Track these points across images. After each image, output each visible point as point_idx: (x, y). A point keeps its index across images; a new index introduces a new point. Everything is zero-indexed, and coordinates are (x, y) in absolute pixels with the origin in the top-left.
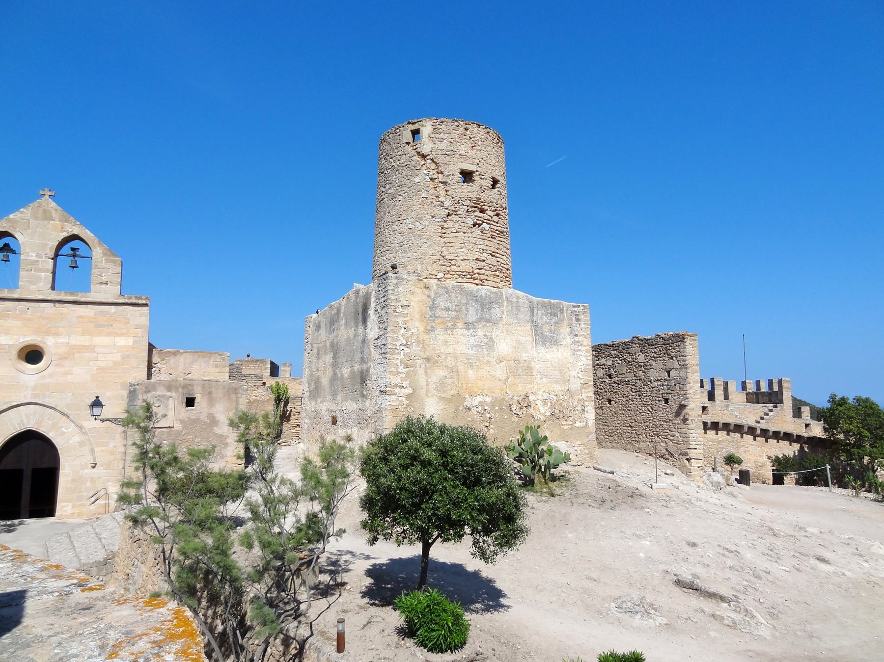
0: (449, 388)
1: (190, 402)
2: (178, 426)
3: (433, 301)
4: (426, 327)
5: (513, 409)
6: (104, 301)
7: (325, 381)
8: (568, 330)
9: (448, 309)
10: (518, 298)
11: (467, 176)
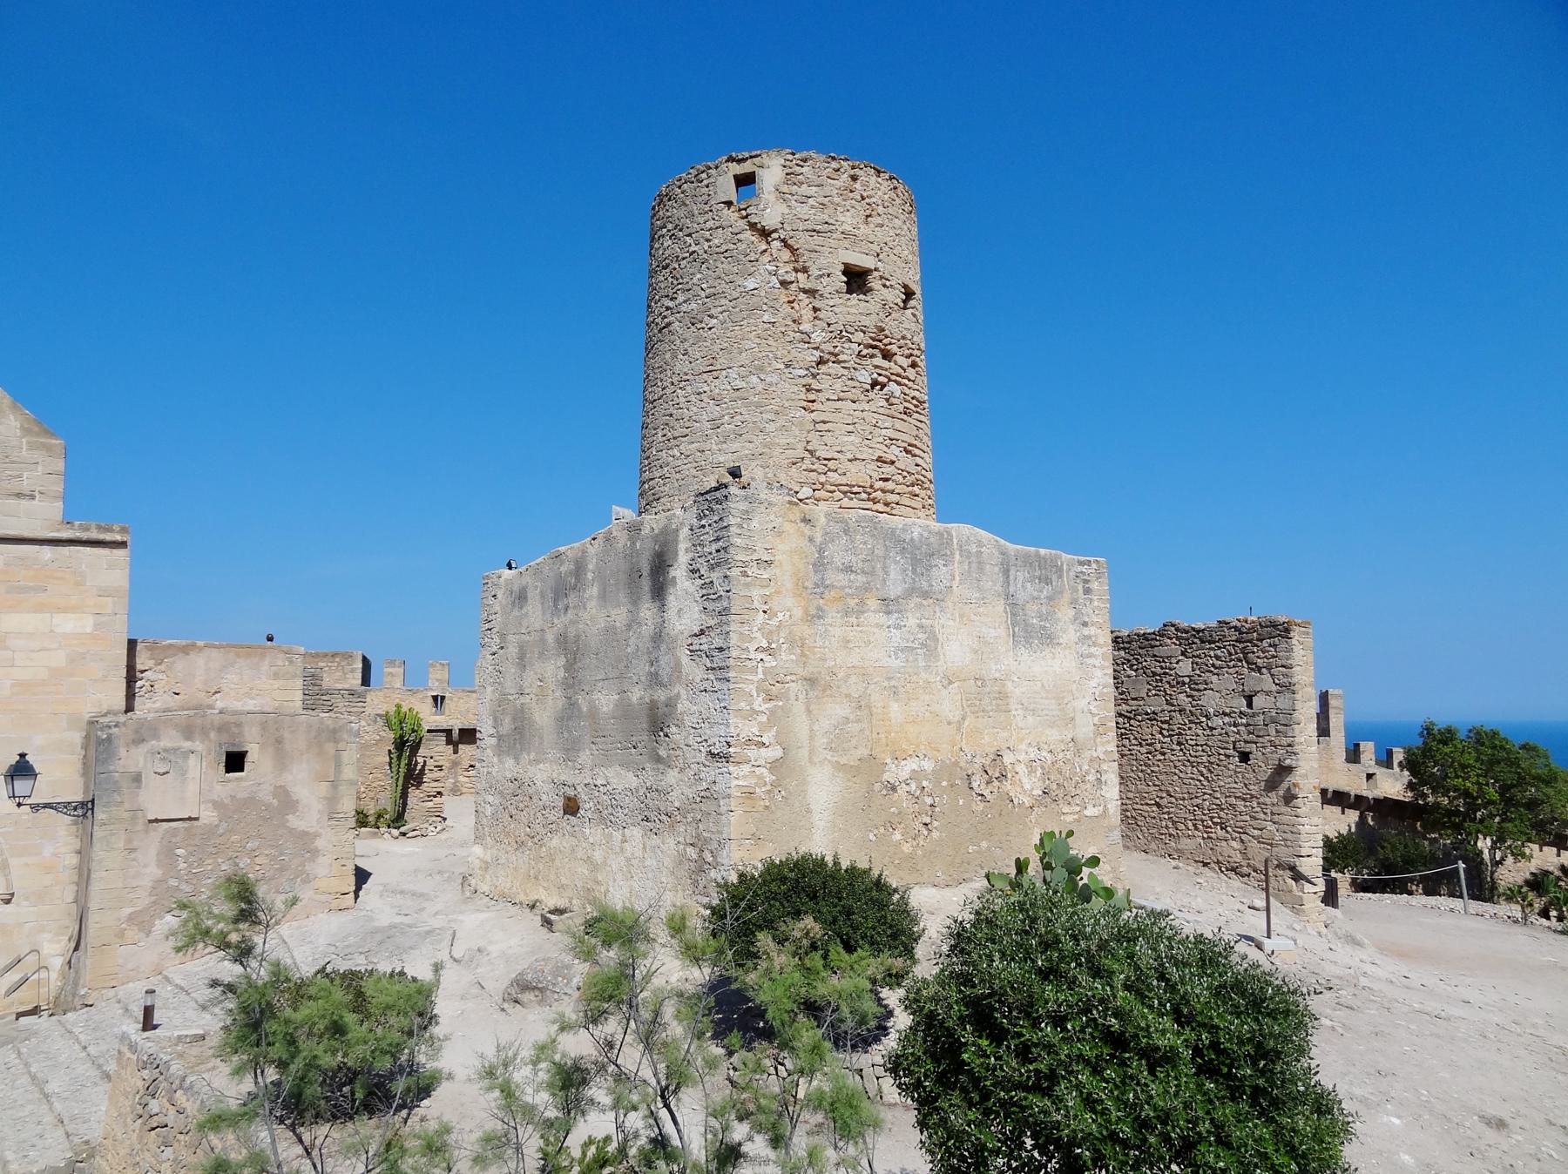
0: (854, 741)
1: (235, 762)
2: (208, 816)
3: (821, 551)
5: (975, 785)
6: (27, 534)
7: (543, 717)
8: (1071, 613)
9: (848, 569)
10: (980, 544)
11: (856, 279)
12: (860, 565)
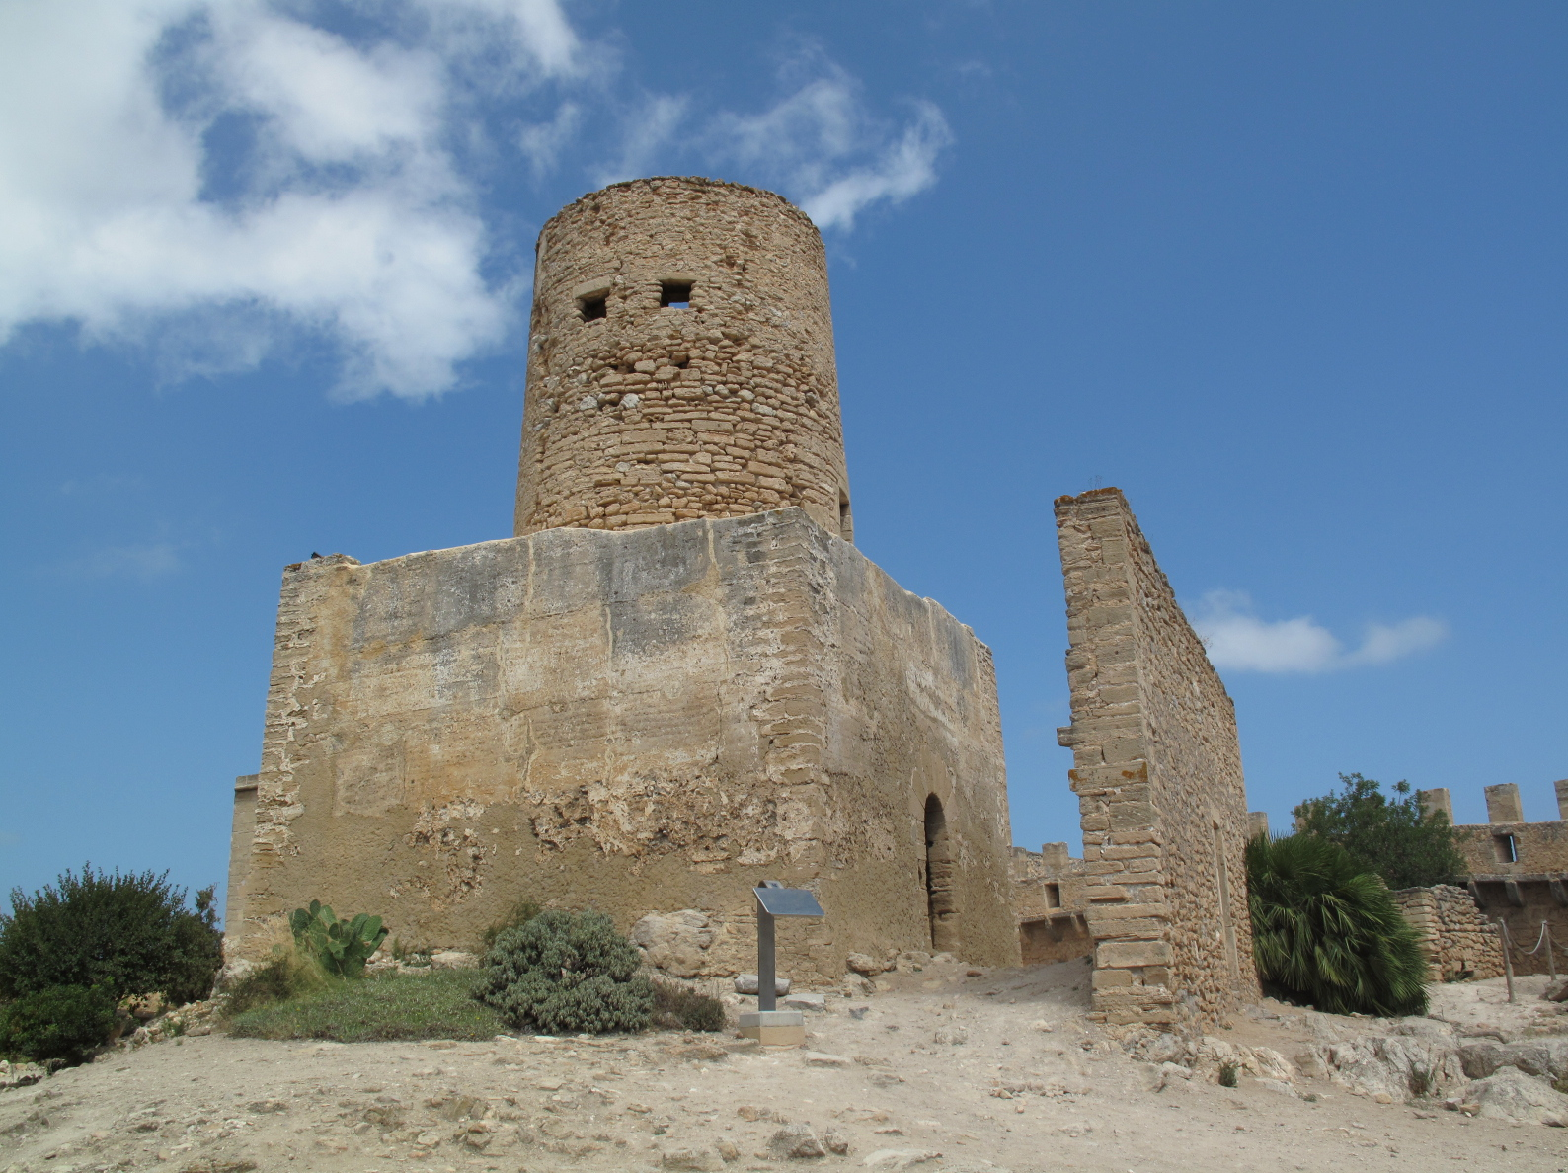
0: (381, 793)
3: (362, 607)
4: (342, 666)
5: (541, 830)
12: (407, 609)
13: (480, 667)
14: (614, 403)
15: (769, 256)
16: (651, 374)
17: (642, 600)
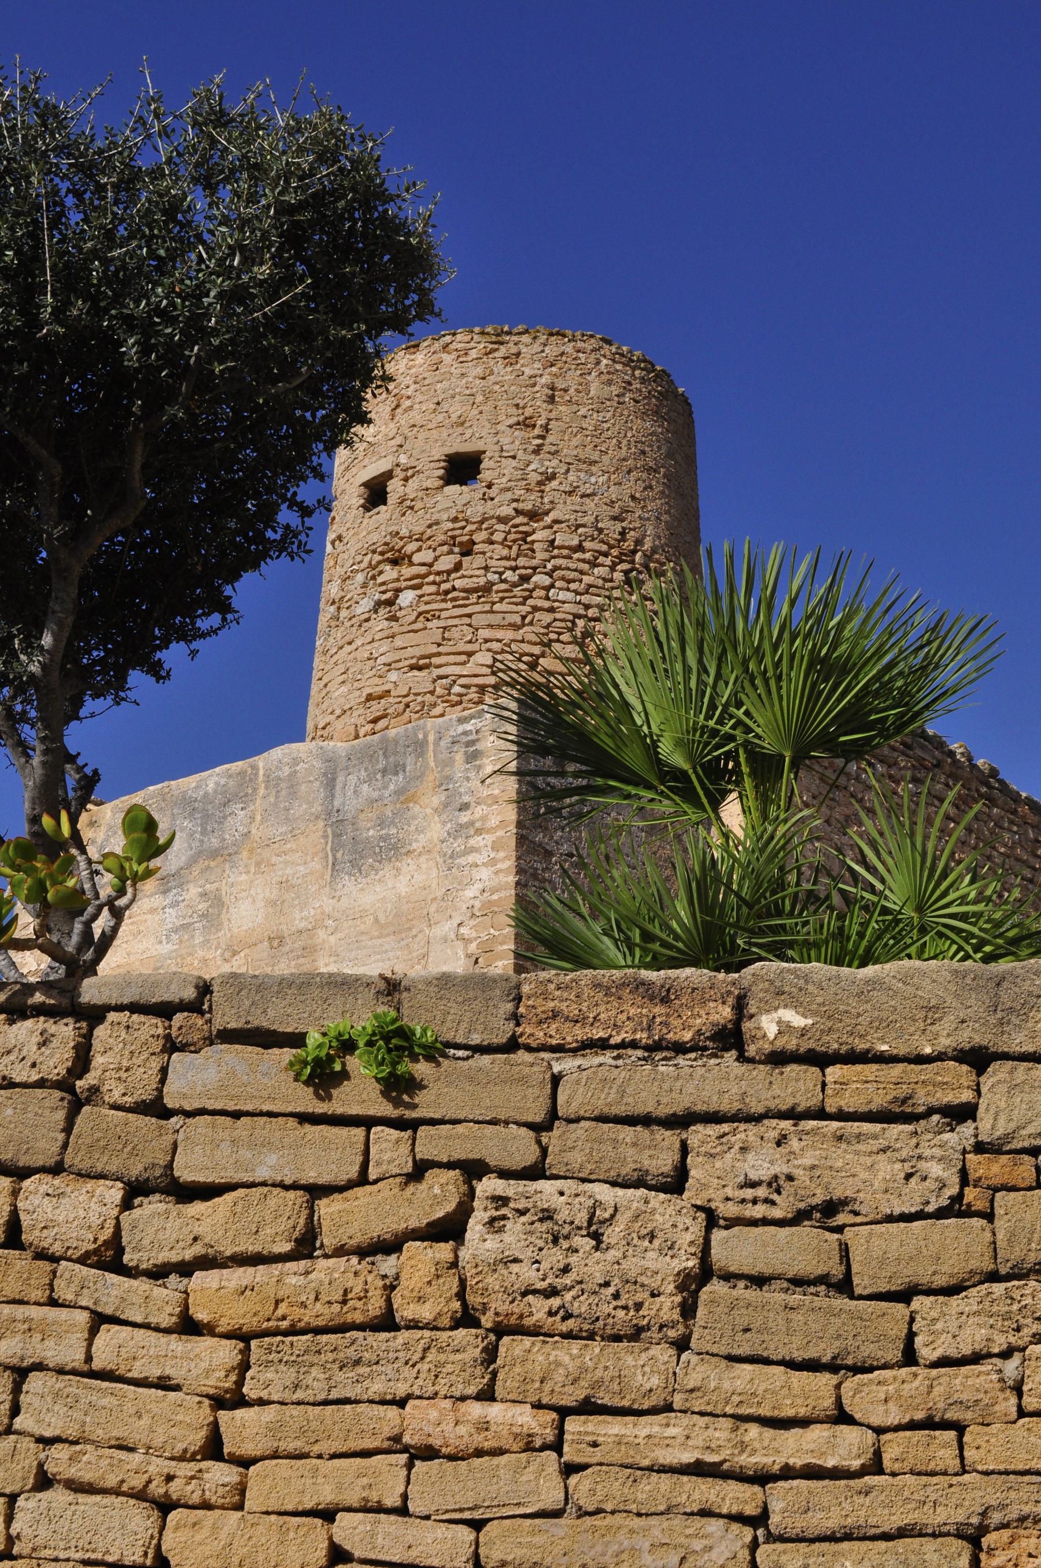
13: (206, 905)
14: (390, 603)
15: (583, 411)
16: (431, 565)
17: (362, 816)
